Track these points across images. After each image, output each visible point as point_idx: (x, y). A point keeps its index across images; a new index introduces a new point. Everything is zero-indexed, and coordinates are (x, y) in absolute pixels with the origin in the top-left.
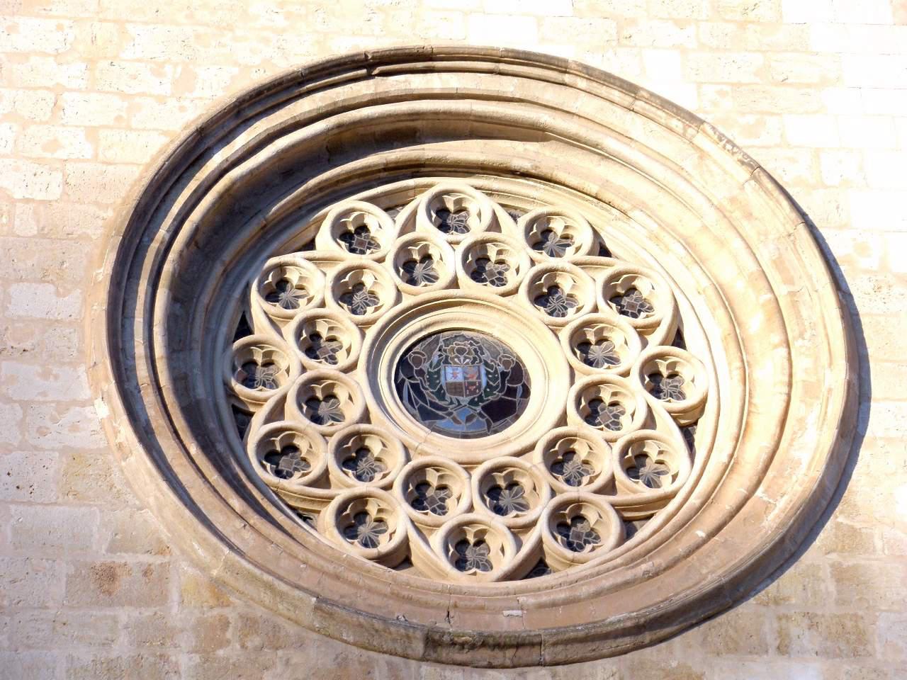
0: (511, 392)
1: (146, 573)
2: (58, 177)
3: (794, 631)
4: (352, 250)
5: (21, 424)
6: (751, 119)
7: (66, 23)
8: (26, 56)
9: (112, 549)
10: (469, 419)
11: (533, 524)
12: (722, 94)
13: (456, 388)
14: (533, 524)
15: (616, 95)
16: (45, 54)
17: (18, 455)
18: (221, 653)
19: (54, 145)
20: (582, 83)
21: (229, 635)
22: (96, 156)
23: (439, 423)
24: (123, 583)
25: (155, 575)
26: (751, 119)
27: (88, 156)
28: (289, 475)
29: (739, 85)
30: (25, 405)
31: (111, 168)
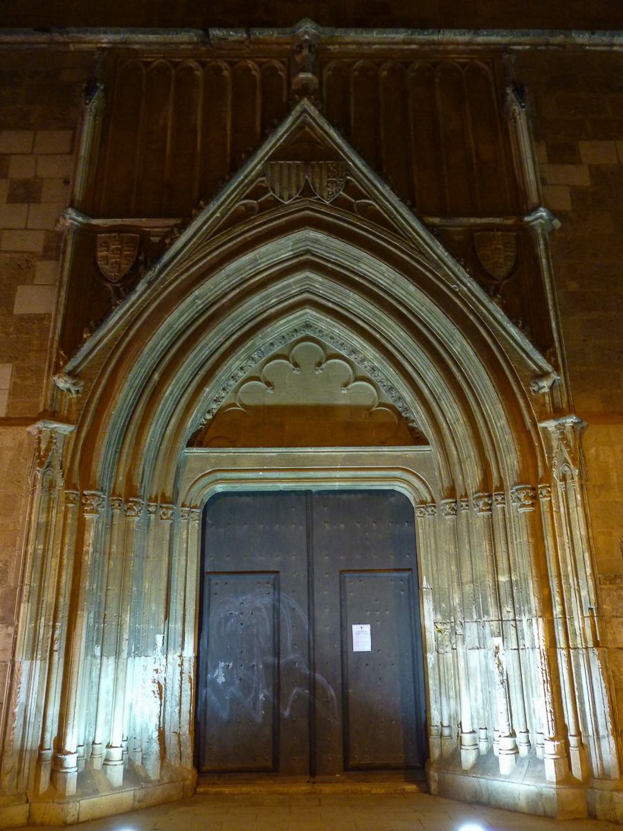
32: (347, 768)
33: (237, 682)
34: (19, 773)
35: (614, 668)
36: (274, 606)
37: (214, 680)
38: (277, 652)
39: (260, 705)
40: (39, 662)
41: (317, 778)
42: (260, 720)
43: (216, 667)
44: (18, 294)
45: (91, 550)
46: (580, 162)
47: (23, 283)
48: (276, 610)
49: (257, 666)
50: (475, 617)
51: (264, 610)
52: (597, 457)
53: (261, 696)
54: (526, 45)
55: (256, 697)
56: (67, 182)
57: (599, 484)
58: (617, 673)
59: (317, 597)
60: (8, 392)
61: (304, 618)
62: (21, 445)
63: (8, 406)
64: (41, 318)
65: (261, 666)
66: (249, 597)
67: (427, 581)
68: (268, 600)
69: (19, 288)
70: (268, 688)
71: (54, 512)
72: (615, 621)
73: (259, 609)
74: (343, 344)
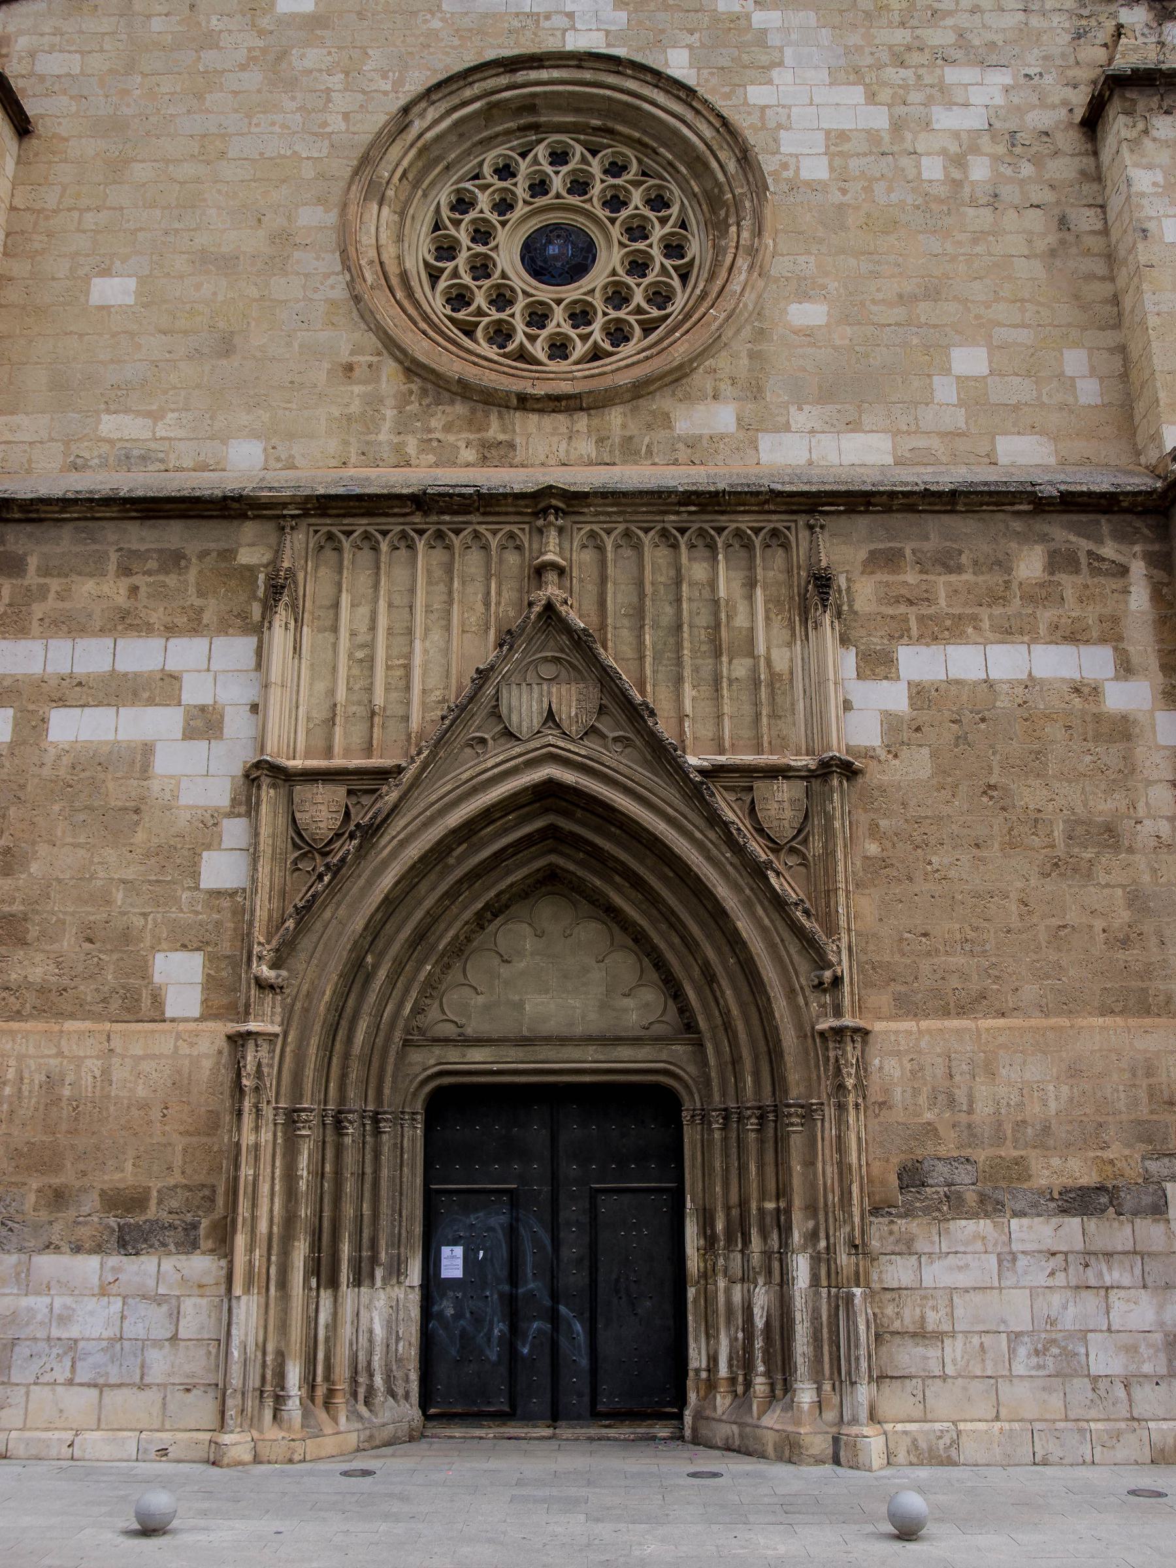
0: (586, 258)
1: (370, 366)
2: (326, 143)
3: (722, 386)
4: (500, 179)
5: (304, 287)
6: (727, 89)
7: (333, 50)
8: (311, 72)
9: (352, 353)
10: (560, 275)
11: (591, 333)
12: (712, 74)
13: (555, 258)
14: (591, 333)
15: (649, 78)
16: (320, 71)
17: (302, 304)
18: (408, 408)
19: (325, 124)
20: (629, 72)
21: (413, 398)
22: (347, 130)
23: (544, 278)
24: (357, 373)
25: (374, 367)
26: (727, 89)
27: (343, 128)
28: (459, 311)
29: (723, 68)
30: (306, 275)
31: (356, 136)
32: (592, 1415)
33: (468, 1315)
34: (243, 1411)
35: (877, 1310)
36: (511, 1225)
37: (441, 1313)
38: (514, 1277)
39: (495, 1341)
40: (255, 1297)
41: (559, 1423)
42: (494, 1358)
43: (443, 1295)
44: (203, 863)
45: (305, 1174)
46: (898, 678)
47: (208, 847)
48: (512, 1232)
49: (492, 1295)
50: (740, 1245)
51: (500, 1231)
52: (881, 1068)
53: (496, 1331)
54: (839, 505)
55: (491, 1330)
56: (254, 708)
57: (881, 1100)
58: (879, 1316)
59: (563, 1215)
60: (199, 988)
61: (547, 1242)
62: (220, 1052)
63: (202, 1003)
64: (233, 894)
65: (496, 1296)
66: (481, 1214)
67: (692, 1201)
68: (504, 1219)
69: (205, 854)
70: (504, 1322)
71: (263, 1131)
72: (883, 1259)
73: (491, 1229)
74: (598, 900)
